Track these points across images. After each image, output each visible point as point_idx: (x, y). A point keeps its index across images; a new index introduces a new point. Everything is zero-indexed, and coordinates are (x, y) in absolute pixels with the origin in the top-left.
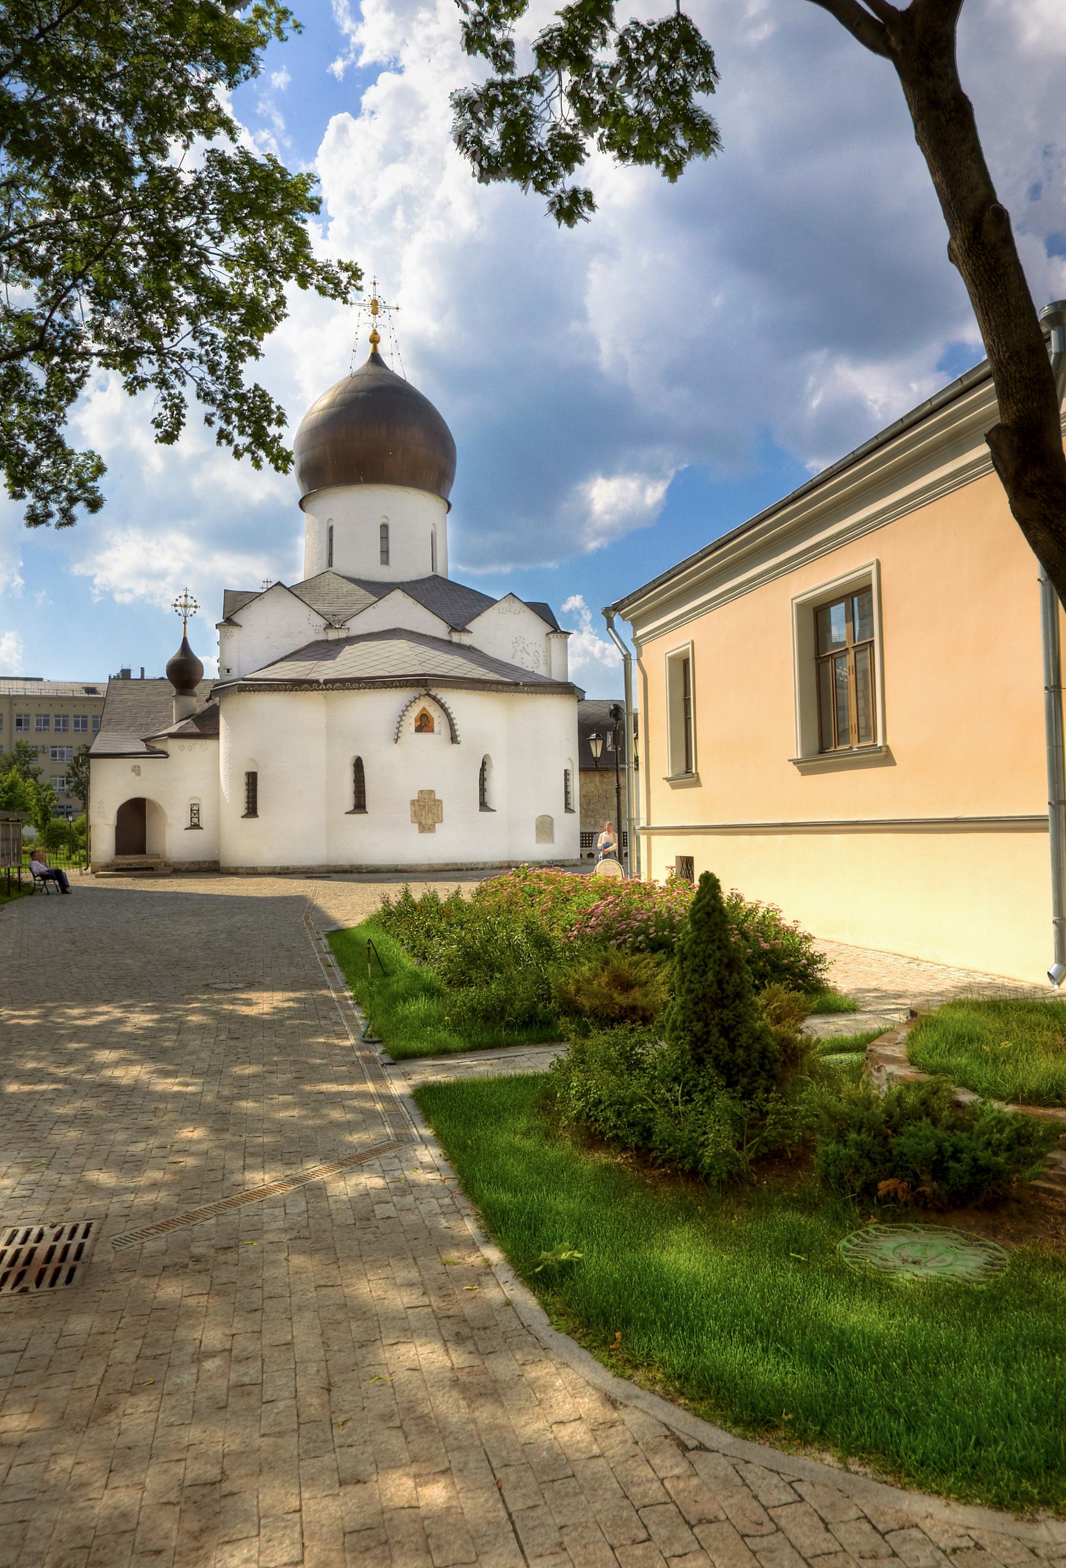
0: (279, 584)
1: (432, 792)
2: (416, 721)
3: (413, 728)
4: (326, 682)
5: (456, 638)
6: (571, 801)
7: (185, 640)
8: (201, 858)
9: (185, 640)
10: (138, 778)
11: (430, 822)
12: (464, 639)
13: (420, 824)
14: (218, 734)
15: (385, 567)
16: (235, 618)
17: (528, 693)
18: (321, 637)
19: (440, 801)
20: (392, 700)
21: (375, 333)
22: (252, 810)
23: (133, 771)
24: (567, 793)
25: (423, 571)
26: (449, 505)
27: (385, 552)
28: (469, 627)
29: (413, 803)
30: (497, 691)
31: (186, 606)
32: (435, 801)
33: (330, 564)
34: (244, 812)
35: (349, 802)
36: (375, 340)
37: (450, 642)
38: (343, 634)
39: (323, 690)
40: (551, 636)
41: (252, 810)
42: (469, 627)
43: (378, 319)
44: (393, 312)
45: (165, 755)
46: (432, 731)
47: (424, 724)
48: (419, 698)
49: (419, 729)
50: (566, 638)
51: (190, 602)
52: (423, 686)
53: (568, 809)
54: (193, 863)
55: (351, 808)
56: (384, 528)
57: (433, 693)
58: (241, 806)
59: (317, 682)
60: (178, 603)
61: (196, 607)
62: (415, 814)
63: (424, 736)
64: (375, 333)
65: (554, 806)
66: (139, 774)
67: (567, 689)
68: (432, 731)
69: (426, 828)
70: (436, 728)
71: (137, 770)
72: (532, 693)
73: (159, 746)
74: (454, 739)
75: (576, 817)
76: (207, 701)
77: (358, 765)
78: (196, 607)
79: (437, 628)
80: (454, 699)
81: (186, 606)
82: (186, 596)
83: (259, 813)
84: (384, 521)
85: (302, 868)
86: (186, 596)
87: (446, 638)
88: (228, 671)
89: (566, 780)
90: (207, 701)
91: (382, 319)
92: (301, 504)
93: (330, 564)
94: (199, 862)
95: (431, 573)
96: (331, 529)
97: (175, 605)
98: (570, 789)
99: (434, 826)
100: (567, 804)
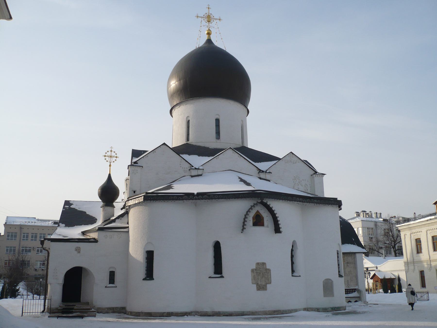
0: (164, 144)
1: (264, 264)
2: (253, 218)
3: (251, 223)
4: (199, 194)
7: (110, 175)
9: (110, 175)
11: (264, 284)
13: (257, 284)
15: (218, 141)
17: (317, 203)
19: (269, 270)
21: (209, 30)
22: (149, 274)
23: (76, 250)
27: (218, 133)
29: (253, 271)
30: (300, 201)
31: (111, 157)
32: (266, 269)
36: (209, 34)
39: (196, 199)
40: (314, 175)
41: (149, 274)
43: (210, 24)
44: (218, 21)
46: (262, 224)
47: (258, 221)
48: (256, 204)
49: (255, 224)
51: (113, 154)
52: (258, 197)
53: (340, 276)
56: (217, 121)
57: (265, 201)
58: (142, 272)
59: (193, 194)
60: (106, 155)
61: (116, 157)
64: (209, 30)
65: (333, 275)
66: (79, 252)
67: (336, 203)
69: (261, 287)
71: (78, 250)
74: (277, 230)
76: (122, 209)
77: (217, 247)
78: (116, 157)
80: (278, 206)
81: (111, 157)
82: (111, 151)
83: (154, 277)
84: (217, 117)
86: (111, 151)
88: (134, 192)
90: (122, 209)
91: (213, 24)
93: (188, 139)
96: (188, 122)
97: (105, 156)
99: (266, 287)
100: (339, 272)
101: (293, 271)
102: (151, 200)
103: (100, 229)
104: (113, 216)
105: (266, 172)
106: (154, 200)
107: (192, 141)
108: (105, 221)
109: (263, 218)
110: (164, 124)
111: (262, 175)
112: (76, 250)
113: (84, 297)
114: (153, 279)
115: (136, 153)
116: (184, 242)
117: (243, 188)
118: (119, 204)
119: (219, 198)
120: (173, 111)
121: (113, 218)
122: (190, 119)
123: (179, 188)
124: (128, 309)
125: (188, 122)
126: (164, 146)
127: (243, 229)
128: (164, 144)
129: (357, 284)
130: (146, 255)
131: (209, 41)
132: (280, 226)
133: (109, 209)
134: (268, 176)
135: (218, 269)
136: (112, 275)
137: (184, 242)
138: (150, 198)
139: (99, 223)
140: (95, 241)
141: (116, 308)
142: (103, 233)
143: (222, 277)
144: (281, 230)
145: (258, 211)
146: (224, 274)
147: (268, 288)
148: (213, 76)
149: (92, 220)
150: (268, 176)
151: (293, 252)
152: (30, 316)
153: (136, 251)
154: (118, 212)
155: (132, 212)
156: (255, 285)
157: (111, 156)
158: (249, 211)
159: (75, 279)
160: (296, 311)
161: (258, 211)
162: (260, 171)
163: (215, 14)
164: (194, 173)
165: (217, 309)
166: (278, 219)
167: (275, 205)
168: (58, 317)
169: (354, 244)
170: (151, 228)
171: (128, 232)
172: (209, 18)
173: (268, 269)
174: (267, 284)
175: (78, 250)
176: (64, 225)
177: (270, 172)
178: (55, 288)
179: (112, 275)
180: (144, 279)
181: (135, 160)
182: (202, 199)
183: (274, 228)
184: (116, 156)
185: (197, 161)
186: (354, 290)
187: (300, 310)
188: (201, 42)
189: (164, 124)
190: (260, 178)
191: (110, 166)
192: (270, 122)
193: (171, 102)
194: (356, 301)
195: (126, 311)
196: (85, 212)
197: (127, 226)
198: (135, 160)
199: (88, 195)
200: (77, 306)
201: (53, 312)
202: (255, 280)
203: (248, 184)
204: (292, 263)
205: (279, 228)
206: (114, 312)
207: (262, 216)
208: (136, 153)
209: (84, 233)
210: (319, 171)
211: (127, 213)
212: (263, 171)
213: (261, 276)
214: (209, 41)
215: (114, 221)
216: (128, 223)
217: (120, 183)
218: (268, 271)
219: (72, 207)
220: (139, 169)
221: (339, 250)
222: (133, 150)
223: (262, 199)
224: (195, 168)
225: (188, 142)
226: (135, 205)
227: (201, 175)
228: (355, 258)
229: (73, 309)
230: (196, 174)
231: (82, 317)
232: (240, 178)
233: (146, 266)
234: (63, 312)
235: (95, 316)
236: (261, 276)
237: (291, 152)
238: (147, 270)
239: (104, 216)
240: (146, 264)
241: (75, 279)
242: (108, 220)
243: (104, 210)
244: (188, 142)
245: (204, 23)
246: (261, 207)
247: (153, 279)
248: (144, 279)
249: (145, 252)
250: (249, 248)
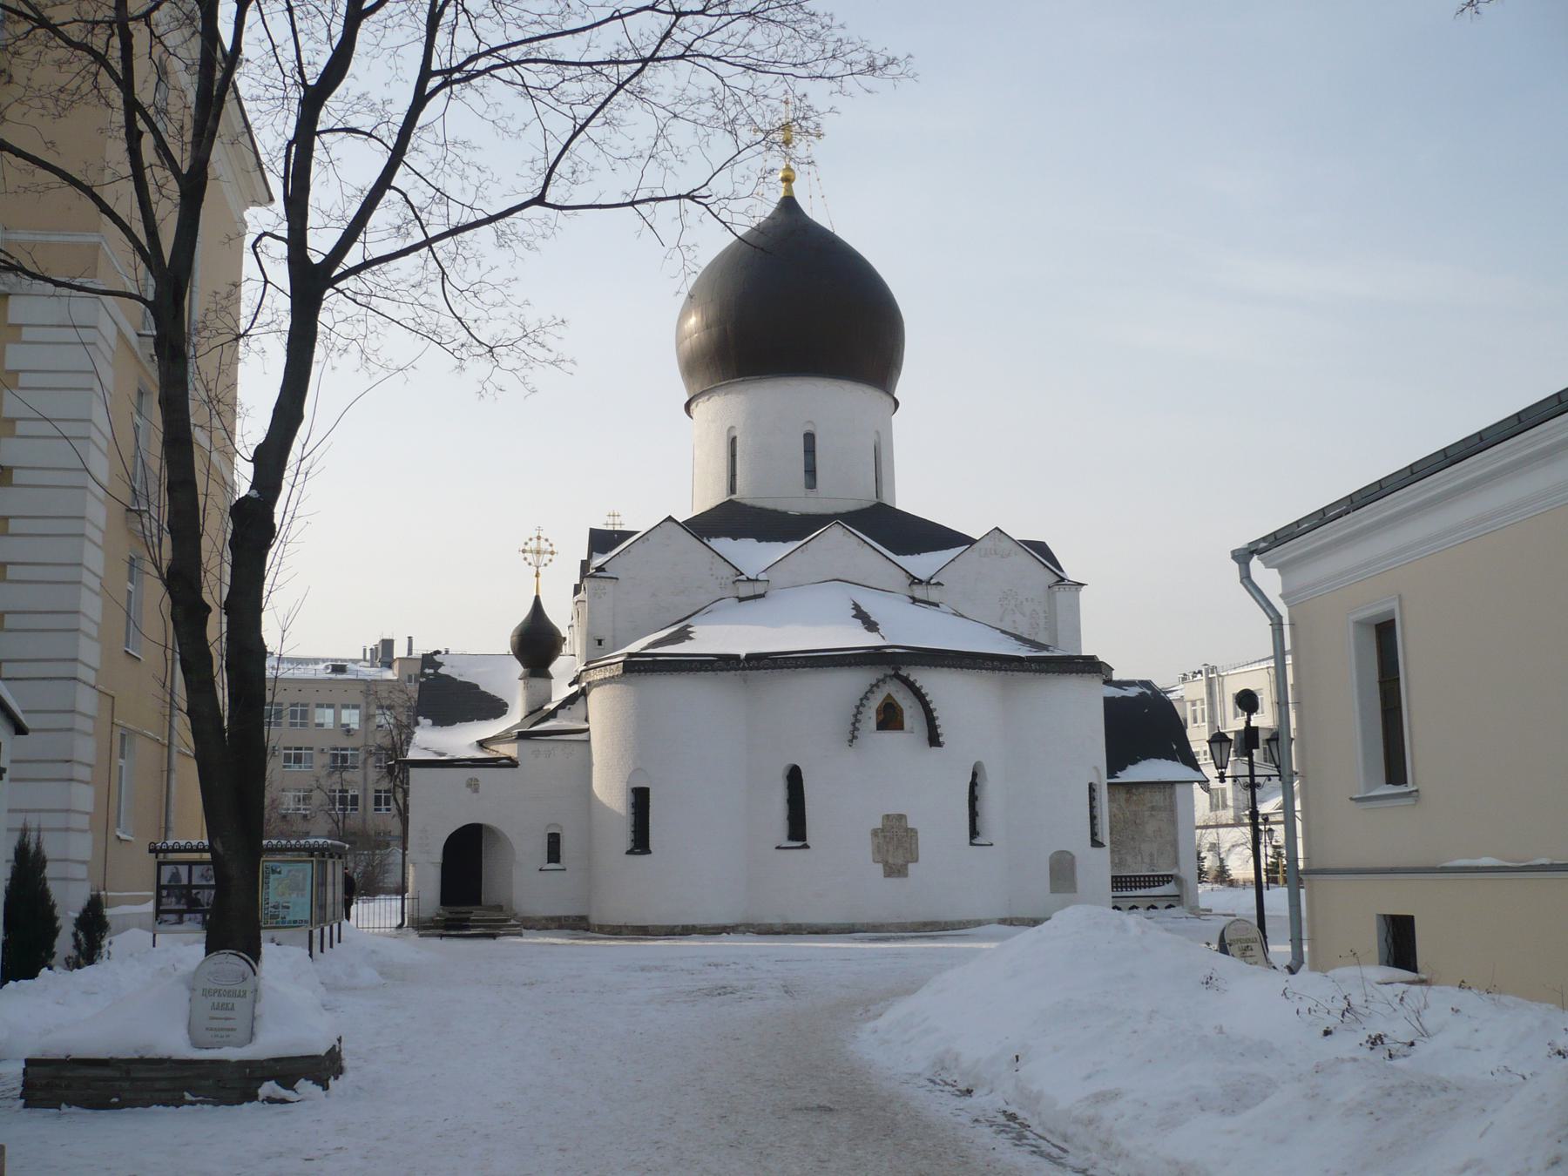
0: (670, 518)
1: (901, 817)
2: (878, 712)
3: (873, 724)
4: (749, 657)
6: (1099, 828)
7: (537, 599)
9: (537, 599)
11: (900, 862)
13: (886, 864)
17: (1036, 671)
19: (914, 831)
20: (854, 682)
21: (788, 168)
22: (641, 842)
23: (469, 785)
24: (1093, 818)
25: (860, 496)
26: (897, 403)
27: (811, 471)
29: (875, 833)
31: (538, 552)
32: (907, 830)
33: (732, 490)
34: (628, 845)
36: (787, 180)
39: (744, 669)
41: (641, 842)
46: (899, 726)
47: (890, 718)
48: (883, 681)
49: (883, 725)
50: (1078, 591)
51: (544, 546)
53: (1096, 843)
56: (810, 439)
57: (903, 672)
58: (625, 838)
59: (736, 657)
63: (889, 736)
66: (476, 791)
67: (1091, 666)
69: (895, 870)
70: (907, 722)
71: (473, 785)
72: (1041, 671)
74: (934, 739)
75: (1107, 850)
77: (794, 778)
78: (552, 553)
81: (538, 552)
84: (809, 428)
88: (600, 642)
89: (1092, 799)
92: (688, 406)
93: (732, 490)
95: (874, 500)
96: (734, 440)
97: (524, 551)
98: (1097, 812)
100: (1094, 834)
101: (974, 832)
102: (639, 671)
103: (523, 736)
104: (549, 700)
105: (928, 583)
106: (646, 671)
107: (744, 494)
108: (531, 713)
109: (901, 711)
110: (668, 453)
111: (919, 592)
112: (469, 785)
113: (487, 896)
115: (602, 541)
116: (718, 770)
117: (860, 639)
118: (564, 668)
119: (797, 667)
120: (693, 406)
121: (551, 707)
122: (737, 433)
123: (709, 639)
124: (595, 919)
125: (733, 441)
127: (853, 738)
128: (670, 518)
129: (1176, 863)
130: (631, 798)
133: (538, 682)
134: (933, 594)
135: (797, 828)
136: (554, 843)
137: (718, 770)
138: (635, 667)
139: (515, 717)
140: (512, 763)
142: (528, 745)
143: (806, 847)
145: (889, 696)
146: (809, 841)
148: (799, 311)
149: (493, 707)
150: (933, 594)
151: (977, 789)
152: (378, 934)
153: (609, 788)
154: (561, 690)
155: (595, 696)
157: (538, 552)
158: (866, 697)
159: (467, 853)
160: (979, 923)
161: (889, 696)
162: (915, 581)
164: (746, 590)
165: (795, 919)
167: (931, 681)
168: (441, 936)
169: (1174, 759)
170: (642, 736)
171: (588, 741)
175: (473, 785)
176: (429, 722)
177: (939, 584)
178: (423, 872)
179: (554, 843)
180: (628, 853)
181: (598, 560)
182: (758, 668)
185: (754, 555)
186: (1167, 879)
187: (989, 922)
188: (764, 208)
189: (668, 453)
190: (915, 600)
192: (941, 444)
193: (689, 387)
194: (1169, 907)
196: (476, 687)
197: (585, 726)
198: (598, 560)
199: (479, 639)
200: (476, 914)
201: (423, 926)
202: (880, 854)
203: (871, 626)
205: (938, 735)
206: (560, 927)
208: (602, 541)
209: (482, 744)
210: (1071, 573)
211: (584, 693)
212: (921, 582)
213: (896, 844)
215: (552, 714)
216: (587, 720)
217: (561, 614)
218: (912, 834)
219: (442, 671)
220: (609, 585)
221: (1095, 781)
222: (593, 533)
223: (897, 669)
224: (749, 580)
226: (605, 681)
227: (762, 596)
228: (1172, 795)
229: (468, 919)
230: (750, 592)
231: (494, 936)
232: (856, 607)
234: (447, 928)
235: (520, 935)
236: (896, 844)
238: (634, 832)
239: (529, 701)
241: (467, 853)
242: (537, 712)
243: (526, 687)
246: (893, 685)
248: (628, 853)
250: (869, 781)
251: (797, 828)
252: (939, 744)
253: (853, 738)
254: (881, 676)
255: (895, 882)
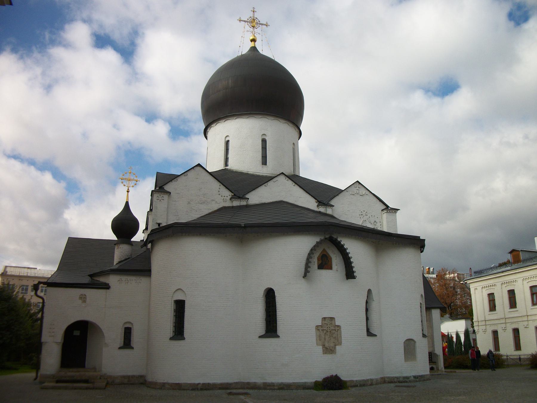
1: (332, 319)
3: (316, 266)
4: (246, 227)
5: (322, 209)
7: (127, 204)
8: (130, 374)
9: (127, 204)
10: (83, 305)
11: (332, 345)
12: (329, 211)
13: (324, 346)
14: (150, 271)
16: (167, 188)
18: (228, 204)
23: (80, 298)
28: (332, 202)
33: (226, 165)
35: (260, 326)
37: (320, 212)
38: (243, 203)
41: (179, 332)
42: (332, 202)
45: (106, 287)
46: (331, 268)
47: (325, 263)
49: (321, 267)
54: (124, 377)
55: (262, 332)
60: (124, 177)
62: (319, 338)
63: (324, 273)
66: (84, 301)
68: (331, 268)
69: (329, 350)
73: (102, 279)
77: (270, 296)
79: (310, 203)
85: (221, 384)
87: (316, 209)
93: (226, 165)
94: (128, 377)
95: (293, 174)
96: (227, 143)
99: (335, 348)
109: (331, 259)
112: (80, 298)
114: (184, 339)
124: (150, 379)
126: (199, 168)
131: (254, 49)
132: (354, 270)
136: (128, 332)
141: (132, 376)
144: (355, 274)
145: (324, 250)
147: (337, 351)
156: (321, 347)
161: (324, 250)
163: (261, 17)
166: (352, 260)
172: (253, 23)
173: (338, 326)
174: (336, 345)
175: (83, 298)
179: (128, 332)
180: (171, 339)
183: (345, 273)
184: (136, 179)
191: (128, 192)
195: (145, 381)
204: (367, 319)
205: (353, 272)
207: (329, 256)
210: (391, 206)
213: (329, 333)
214: (254, 49)
217: (140, 213)
220: (166, 197)
225: (227, 167)
233: (174, 321)
237: (358, 181)
238: (175, 327)
240: (175, 318)
244: (227, 167)
245: (248, 27)
247: (184, 339)
248: (171, 339)
249: (173, 302)
251: (271, 328)
252: (354, 277)
253: (306, 274)
254: (318, 240)
255: (329, 356)
